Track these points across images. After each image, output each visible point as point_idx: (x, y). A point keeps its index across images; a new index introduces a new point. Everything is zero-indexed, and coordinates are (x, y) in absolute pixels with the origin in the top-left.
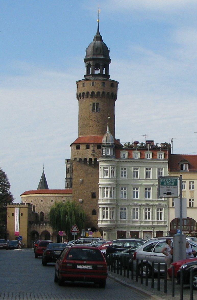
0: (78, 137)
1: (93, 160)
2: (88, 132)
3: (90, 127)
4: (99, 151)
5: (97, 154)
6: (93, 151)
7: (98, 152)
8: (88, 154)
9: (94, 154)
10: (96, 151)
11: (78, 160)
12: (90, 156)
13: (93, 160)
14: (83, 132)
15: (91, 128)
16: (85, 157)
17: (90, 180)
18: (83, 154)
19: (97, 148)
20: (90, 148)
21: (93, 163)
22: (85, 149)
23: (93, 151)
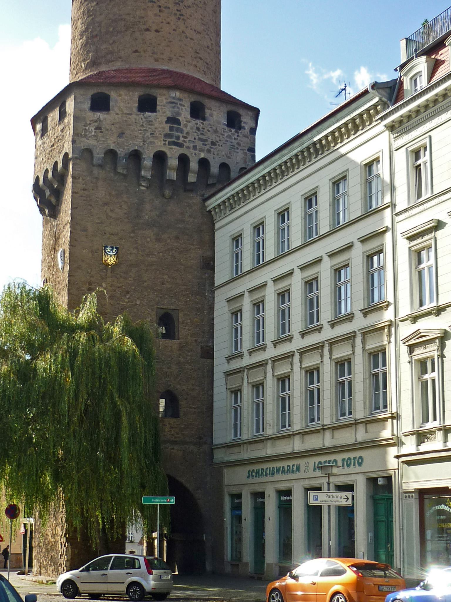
0: (67, 83)
1: (173, 162)
2: (136, 51)
3: (147, 30)
4: (198, 129)
5: (190, 138)
6: (173, 121)
7: (192, 128)
8: (148, 134)
9: (178, 138)
10: (186, 126)
11: (99, 155)
12: (160, 145)
13: (173, 162)
14: (111, 53)
15: (149, 36)
16: (135, 145)
17: (148, 255)
18: (123, 133)
19: (189, 110)
20: (158, 108)
21: (172, 175)
22: (135, 110)
23: (173, 121)
